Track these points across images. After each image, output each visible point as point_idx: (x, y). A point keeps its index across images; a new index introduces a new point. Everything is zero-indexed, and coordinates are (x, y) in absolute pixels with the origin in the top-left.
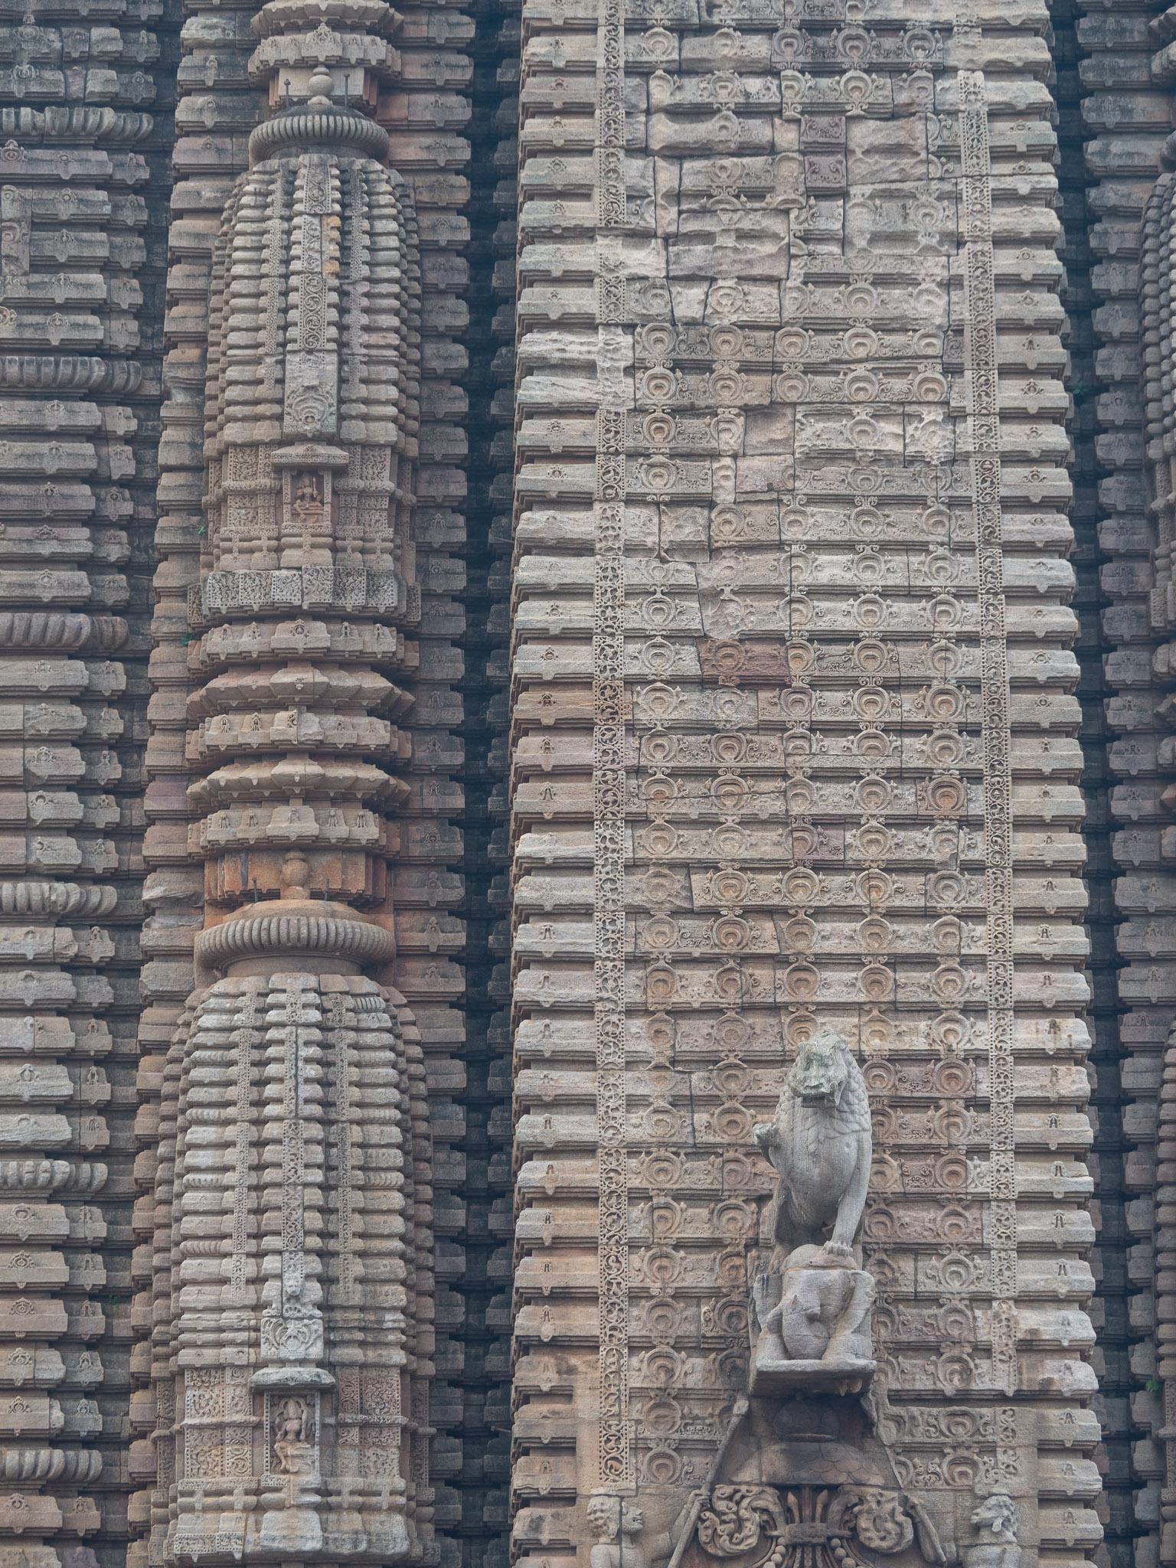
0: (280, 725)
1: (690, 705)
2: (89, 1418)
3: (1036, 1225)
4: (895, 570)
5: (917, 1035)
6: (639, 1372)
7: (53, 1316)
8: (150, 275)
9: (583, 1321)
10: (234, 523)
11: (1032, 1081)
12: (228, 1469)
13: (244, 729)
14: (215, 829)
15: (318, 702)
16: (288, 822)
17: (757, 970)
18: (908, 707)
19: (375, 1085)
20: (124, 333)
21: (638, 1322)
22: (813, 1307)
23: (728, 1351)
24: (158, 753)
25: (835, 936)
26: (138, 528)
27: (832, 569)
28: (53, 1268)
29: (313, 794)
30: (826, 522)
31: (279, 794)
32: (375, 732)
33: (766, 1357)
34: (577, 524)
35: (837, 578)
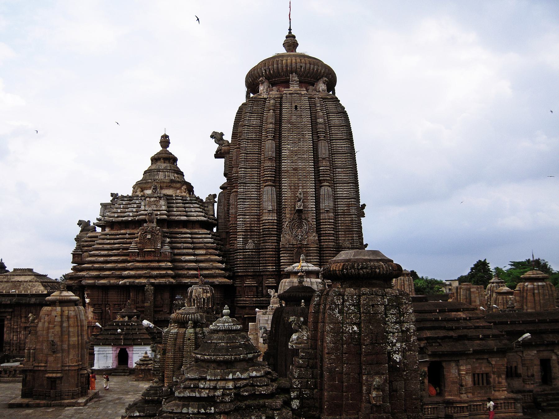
1: (292, 171)
3: (312, 201)
4: (303, 164)
5: (305, 190)
11: (311, 193)
13: (267, 173)
15: (270, 171)
16: (269, 178)
17: (296, 187)
18: (304, 172)
22: (299, 206)
23: (295, 208)
25: (300, 185)
26: (260, 162)
27: (300, 164)
30: (300, 161)
33: (297, 208)
34: (286, 161)
35: (300, 164)
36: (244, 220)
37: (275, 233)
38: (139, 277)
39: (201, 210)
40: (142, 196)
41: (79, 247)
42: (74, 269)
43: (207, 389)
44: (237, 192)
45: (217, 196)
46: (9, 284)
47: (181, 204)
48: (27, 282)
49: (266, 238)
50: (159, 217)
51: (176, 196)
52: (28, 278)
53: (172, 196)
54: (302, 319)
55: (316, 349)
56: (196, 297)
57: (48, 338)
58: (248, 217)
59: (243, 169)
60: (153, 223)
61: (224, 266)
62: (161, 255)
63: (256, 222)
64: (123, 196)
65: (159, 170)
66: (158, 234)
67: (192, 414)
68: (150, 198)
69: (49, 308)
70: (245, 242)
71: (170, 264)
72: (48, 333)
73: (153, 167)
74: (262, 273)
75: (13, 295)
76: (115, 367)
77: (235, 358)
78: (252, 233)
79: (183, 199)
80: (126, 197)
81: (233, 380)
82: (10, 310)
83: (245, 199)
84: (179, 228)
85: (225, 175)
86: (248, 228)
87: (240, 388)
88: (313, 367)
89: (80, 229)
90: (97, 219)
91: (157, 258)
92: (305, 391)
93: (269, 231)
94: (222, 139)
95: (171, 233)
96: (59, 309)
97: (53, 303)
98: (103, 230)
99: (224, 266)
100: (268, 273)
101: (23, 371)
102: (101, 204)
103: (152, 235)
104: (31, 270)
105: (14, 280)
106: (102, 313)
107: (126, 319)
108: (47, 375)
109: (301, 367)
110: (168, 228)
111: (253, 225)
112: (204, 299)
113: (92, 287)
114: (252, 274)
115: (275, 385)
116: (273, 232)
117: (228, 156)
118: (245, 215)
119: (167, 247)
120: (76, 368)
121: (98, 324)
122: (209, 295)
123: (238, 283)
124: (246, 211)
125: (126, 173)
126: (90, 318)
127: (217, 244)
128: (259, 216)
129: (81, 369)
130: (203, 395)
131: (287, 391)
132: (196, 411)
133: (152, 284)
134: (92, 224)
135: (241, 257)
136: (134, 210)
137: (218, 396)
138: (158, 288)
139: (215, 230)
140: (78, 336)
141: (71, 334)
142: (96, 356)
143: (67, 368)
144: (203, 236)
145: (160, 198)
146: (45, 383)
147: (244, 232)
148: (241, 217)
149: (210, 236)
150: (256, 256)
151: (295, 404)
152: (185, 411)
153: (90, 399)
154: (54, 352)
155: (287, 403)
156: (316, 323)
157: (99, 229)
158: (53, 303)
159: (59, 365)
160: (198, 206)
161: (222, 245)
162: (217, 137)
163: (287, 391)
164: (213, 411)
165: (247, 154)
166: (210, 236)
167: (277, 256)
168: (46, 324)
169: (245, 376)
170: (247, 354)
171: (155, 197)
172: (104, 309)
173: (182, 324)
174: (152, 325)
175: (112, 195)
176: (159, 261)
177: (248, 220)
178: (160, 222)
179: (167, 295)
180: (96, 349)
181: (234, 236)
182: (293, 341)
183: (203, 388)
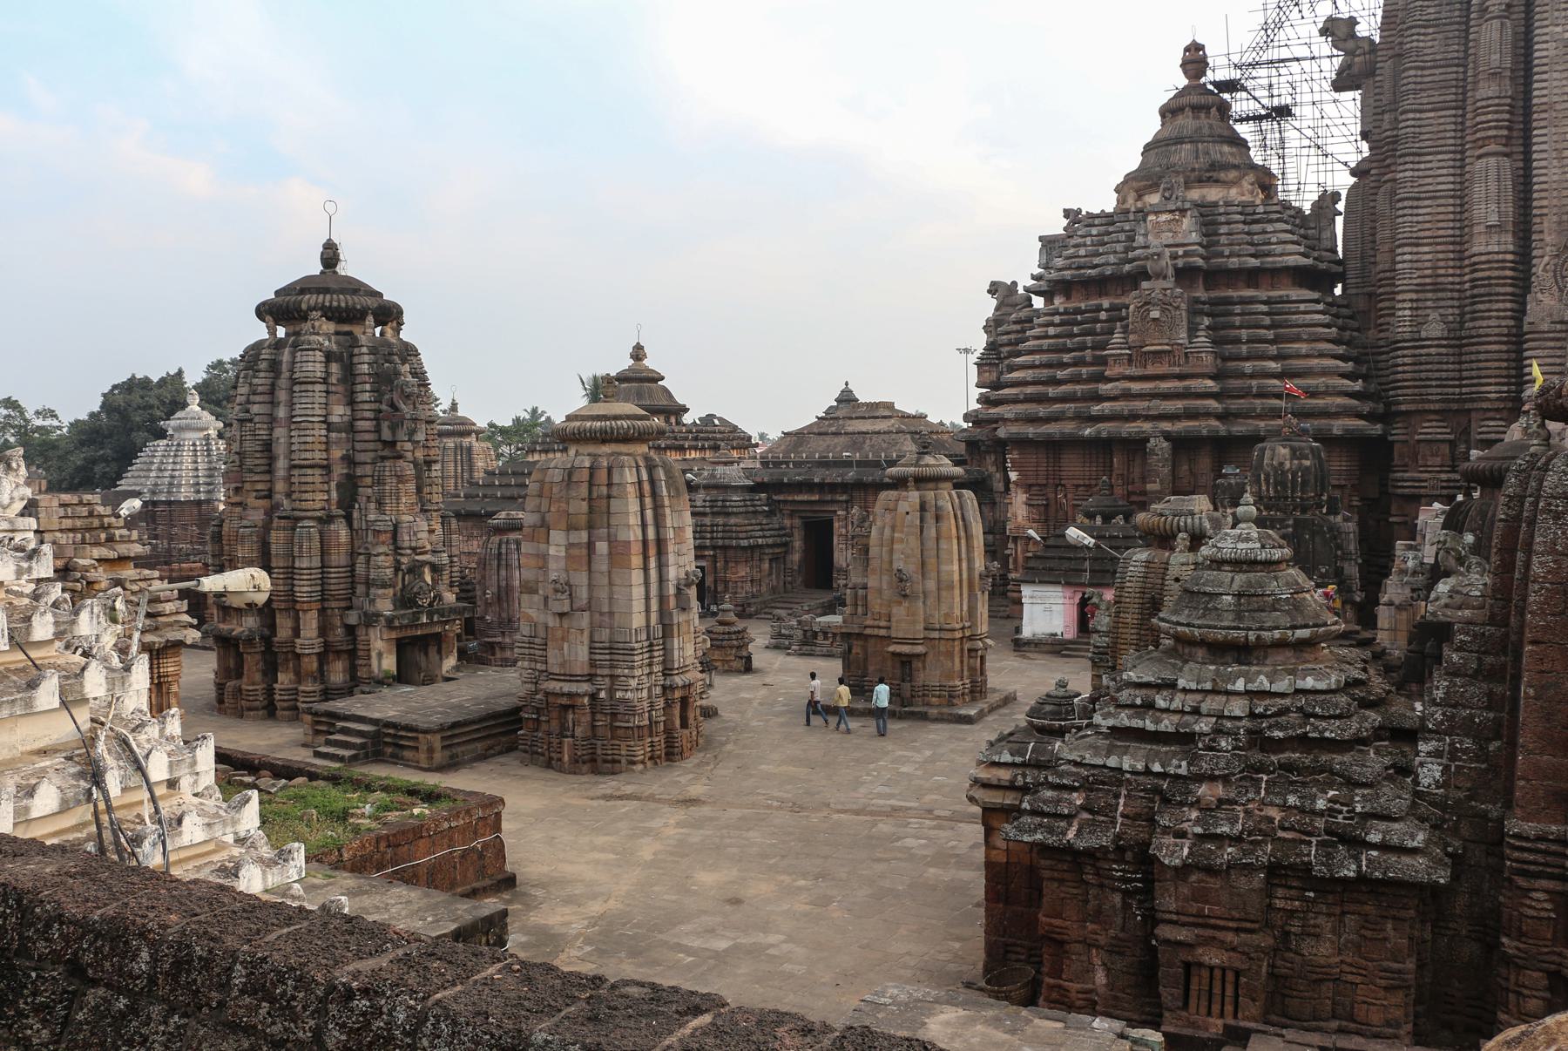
0: (1490, 117)
2: (1458, 232)
6: (1555, 218)
7: (1451, 216)
8: (1466, 44)
9: (1545, 211)
10: (1481, 84)
12: (1483, 239)
13: (1483, 118)
14: (1478, 135)
15: (1496, 112)
16: (1490, 133)
19: (1507, 174)
20: (1461, 55)
21: (1555, 210)
24: (1468, 124)
28: (1451, 209)
29: (1496, 128)
31: (1490, 128)
32: (1507, 116)
36: (1415, 257)
37: (1509, 289)
38: (1133, 417)
39: (1295, 238)
40: (1139, 211)
41: (992, 347)
42: (983, 400)
43: (1175, 712)
44: (1395, 180)
45: (1343, 197)
46: (841, 440)
47: (1241, 226)
48: (878, 433)
49: (1481, 307)
50: (1180, 263)
51: (1227, 204)
52: (882, 426)
53: (1215, 205)
54: (1469, 538)
55: (1507, 625)
56: (1275, 469)
57: (891, 562)
58: (1426, 249)
59: (1411, 115)
60: (1165, 278)
61: (1358, 386)
62: (1187, 362)
63: (1451, 263)
64: (1090, 216)
65: (1179, 140)
66: (1177, 308)
67: (1132, 773)
68: (1156, 213)
69: (893, 494)
70: (1418, 321)
71: (1210, 383)
72: (891, 551)
73: (1166, 134)
74: (1468, 406)
75: (848, 464)
76: (1068, 636)
77: (1258, 637)
78: (1440, 295)
79: (1246, 209)
80: (1097, 216)
81: (1247, 692)
82: (844, 498)
83: (1418, 199)
84: (1235, 288)
85: (1365, 135)
86: (1428, 280)
87: (1262, 716)
88: (1493, 674)
89: (994, 302)
90: (1033, 277)
91: (1177, 370)
92: (1461, 742)
93: (1490, 285)
94: (1353, 35)
95: (1213, 302)
96: (914, 496)
97: (900, 483)
98: (1049, 301)
99: (1358, 386)
100: (1485, 405)
101: (847, 636)
102: (1041, 239)
103: (1163, 311)
104: (890, 406)
105: (850, 429)
106: (1047, 506)
107: (1099, 520)
108: (891, 649)
109: (1455, 674)
110: (1207, 290)
111: (1442, 272)
112: (1294, 475)
113: (1022, 443)
114: (1437, 406)
115: (1374, 717)
116: (1502, 290)
117: (1371, 81)
118: (1417, 245)
119: (1202, 339)
120: (958, 635)
121: (1031, 532)
122: (1307, 463)
123: (1398, 433)
124: (1422, 234)
125: (1096, 155)
126: (1020, 519)
127: (1342, 329)
128: (1460, 241)
129: (970, 638)
130: (1162, 728)
131: (1407, 736)
132: (1140, 766)
133: (1167, 436)
134: (1021, 291)
135: (1407, 360)
136: (1119, 247)
137: (1202, 734)
138: (1183, 445)
139: (1338, 291)
140: (960, 560)
141: (943, 555)
142: (1026, 608)
143: (936, 635)
144: (1302, 307)
145: (1183, 211)
146: (889, 663)
147: (1416, 292)
148: (1407, 249)
149: (1321, 307)
150: (1452, 359)
151: (1430, 774)
152: (1112, 762)
153: (992, 709)
154: (905, 596)
155: (1404, 770)
156: (1508, 551)
157: (1038, 302)
158: (900, 483)
159: (921, 626)
160: (1289, 227)
161: (1358, 330)
162: (1338, 30)
163: (1407, 736)
164: (1183, 771)
165: (1423, 68)
166: (1321, 307)
167: (1513, 356)
168: (887, 531)
169: (1282, 685)
170: (1294, 627)
171: (1171, 212)
172: (1052, 496)
173: (1163, 539)
174: (1089, 541)
175: (1067, 213)
176: (1181, 377)
177: (1429, 257)
178: (1185, 275)
179: (1205, 463)
180: (1027, 591)
181: (1387, 304)
182: (1437, 599)
183: (1167, 710)
